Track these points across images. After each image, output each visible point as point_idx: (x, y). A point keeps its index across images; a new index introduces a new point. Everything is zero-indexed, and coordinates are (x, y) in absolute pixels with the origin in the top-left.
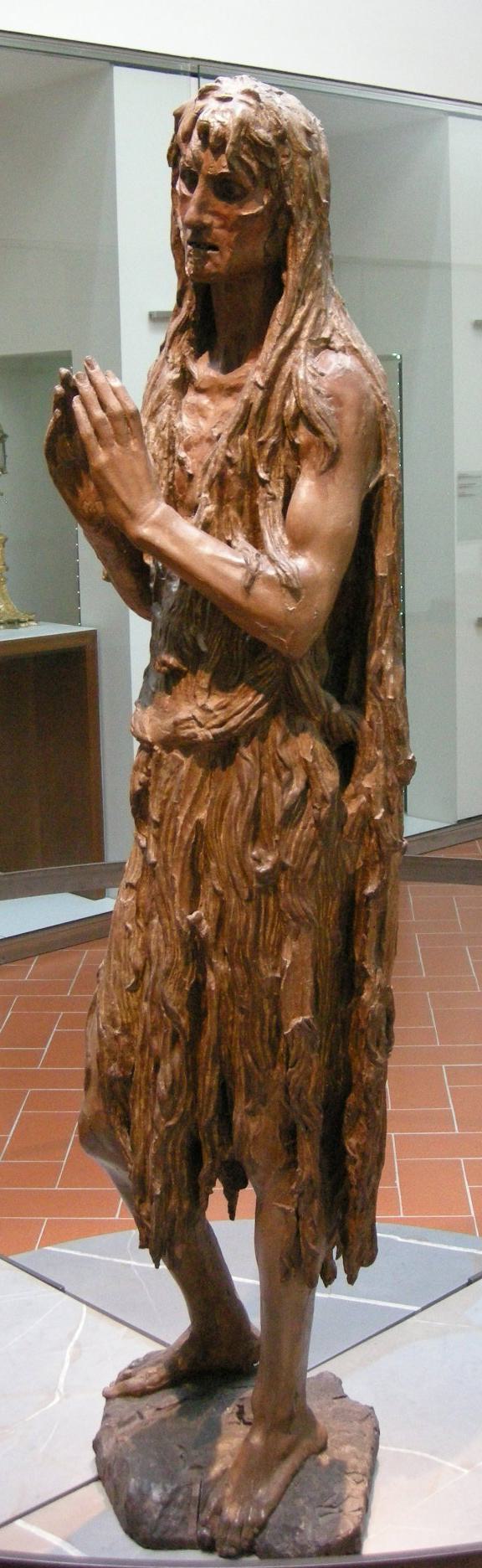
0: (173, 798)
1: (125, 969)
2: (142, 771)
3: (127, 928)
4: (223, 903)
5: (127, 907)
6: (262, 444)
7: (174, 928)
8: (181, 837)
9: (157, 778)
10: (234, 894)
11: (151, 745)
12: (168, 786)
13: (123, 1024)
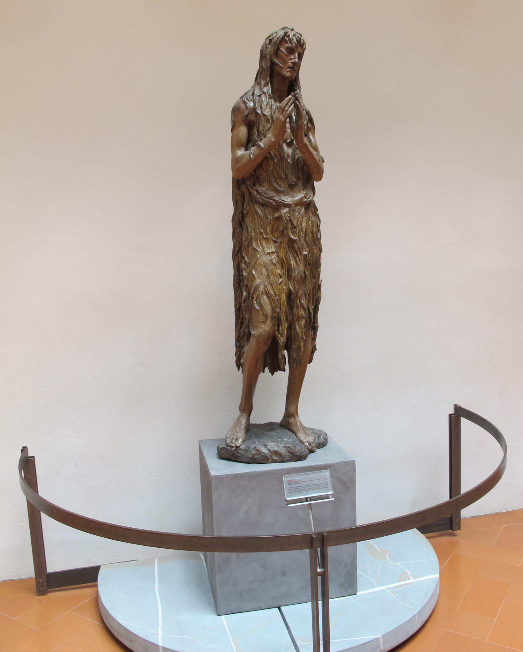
0: (300, 219)
1: (276, 278)
2: (288, 214)
3: (275, 265)
4: (310, 248)
5: (273, 259)
6: (305, 125)
7: (303, 257)
8: (304, 230)
9: (294, 215)
10: (313, 245)
11: (291, 205)
12: (298, 216)
13: (279, 295)
